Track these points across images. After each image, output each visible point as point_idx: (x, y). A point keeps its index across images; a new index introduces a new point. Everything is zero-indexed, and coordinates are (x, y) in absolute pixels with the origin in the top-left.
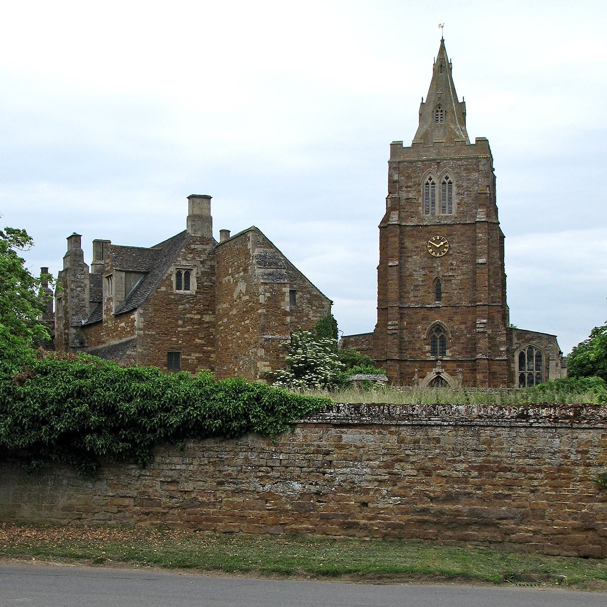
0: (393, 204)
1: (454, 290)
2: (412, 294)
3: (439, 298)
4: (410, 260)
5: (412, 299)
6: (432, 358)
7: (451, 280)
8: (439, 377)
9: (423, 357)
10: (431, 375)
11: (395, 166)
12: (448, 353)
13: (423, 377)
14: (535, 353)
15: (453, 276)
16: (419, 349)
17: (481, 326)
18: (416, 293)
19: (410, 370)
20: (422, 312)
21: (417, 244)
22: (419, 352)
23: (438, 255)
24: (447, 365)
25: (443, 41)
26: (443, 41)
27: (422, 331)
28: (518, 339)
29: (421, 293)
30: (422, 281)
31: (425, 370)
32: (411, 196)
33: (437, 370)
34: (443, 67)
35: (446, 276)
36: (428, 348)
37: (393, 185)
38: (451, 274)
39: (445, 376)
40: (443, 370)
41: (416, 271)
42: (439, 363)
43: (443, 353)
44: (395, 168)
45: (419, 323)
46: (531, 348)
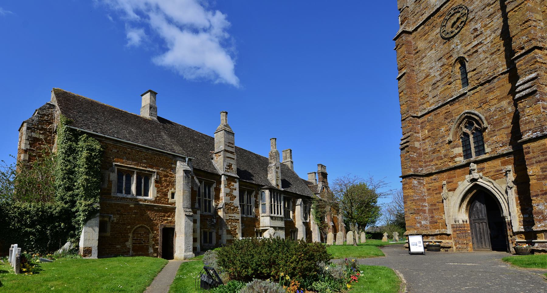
2: (430, 97)
4: (424, 60)
5: (431, 102)
6: (461, 160)
7: (477, 51)
9: (451, 165)
10: (464, 185)
12: (487, 150)
13: (454, 190)
15: (481, 43)
16: (445, 156)
18: (435, 92)
19: (437, 184)
20: (443, 110)
22: (446, 159)
23: (456, 31)
24: (486, 165)
27: (449, 132)
30: (440, 75)
31: (455, 180)
35: (469, 50)
36: (459, 150)
38: (476, 43)
39: (481, 182)
40: (481, 174)
41: (431, 68)
43: (480, 150)
45: (441, 124)
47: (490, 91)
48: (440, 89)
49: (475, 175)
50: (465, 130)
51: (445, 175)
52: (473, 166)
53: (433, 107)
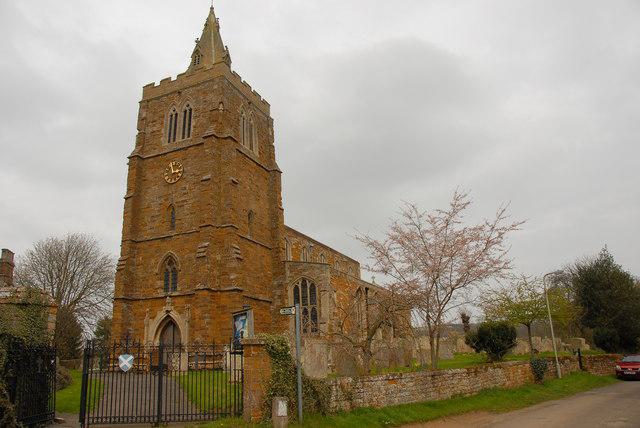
0: (141, 140)
1: (186, 218)
3: (173, 227)
6: (162, 294)
8: (168, 316)
9: (155, 295)
10: (161, 315)
11: (145, 104)
14: (308, 285)
17: (203, 250)
21: (157, 174)
25: (212, 8)
26: (212, 8)
27: (156, 264)
28: (291, 272)
29: (157, 224)
30: (159, 211)
32: (155, 129)
33: (165, 308)
34: (212, 27)
36: (160, 283)
37: (142, 121)
39: (174, 315)
42: (168, 299)
44: (144, 108)
45: (152, 256)
46: (304, 281)
47: (187, 241)
48: (157, 224)
49: (168, 308)
50: (168, 267)
51: (149, 303)
52: (168, 299)
53: (149, 238)
